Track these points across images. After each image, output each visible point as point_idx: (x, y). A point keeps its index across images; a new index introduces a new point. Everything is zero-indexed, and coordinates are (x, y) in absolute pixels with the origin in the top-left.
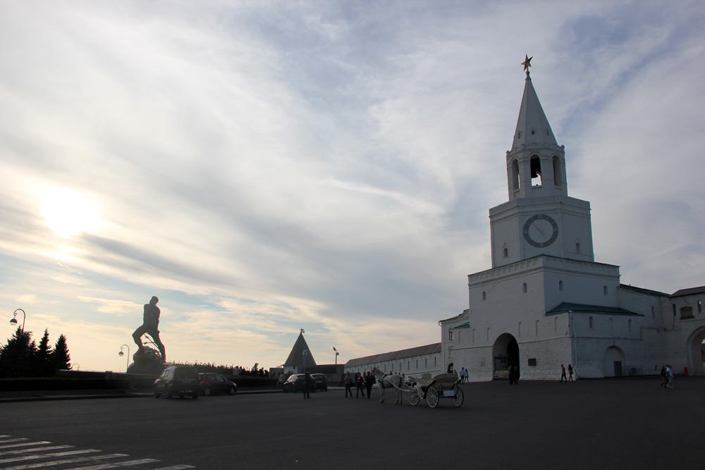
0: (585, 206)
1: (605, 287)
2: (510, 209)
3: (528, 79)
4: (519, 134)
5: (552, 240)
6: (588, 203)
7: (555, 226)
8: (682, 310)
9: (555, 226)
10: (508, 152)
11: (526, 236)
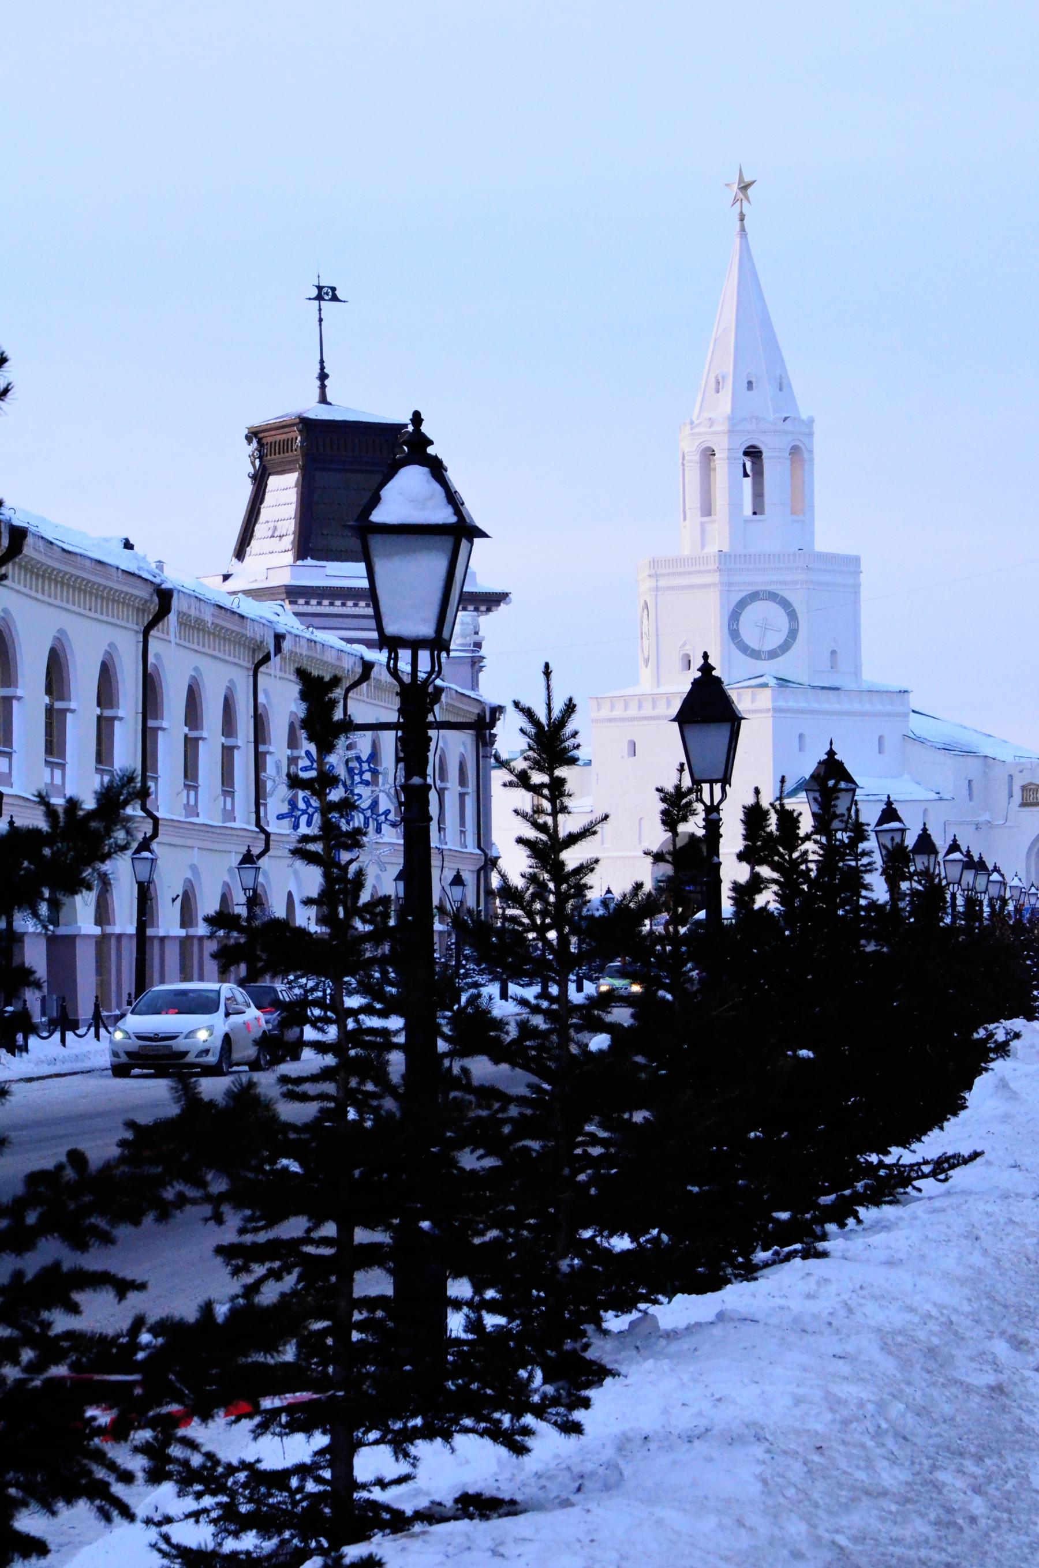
0: (851, 564)
1: (881, 738)
5: (785, 647)
6: (856, 560)
7: (792, 615)
8: (1024, 788)
9: (792, 615)
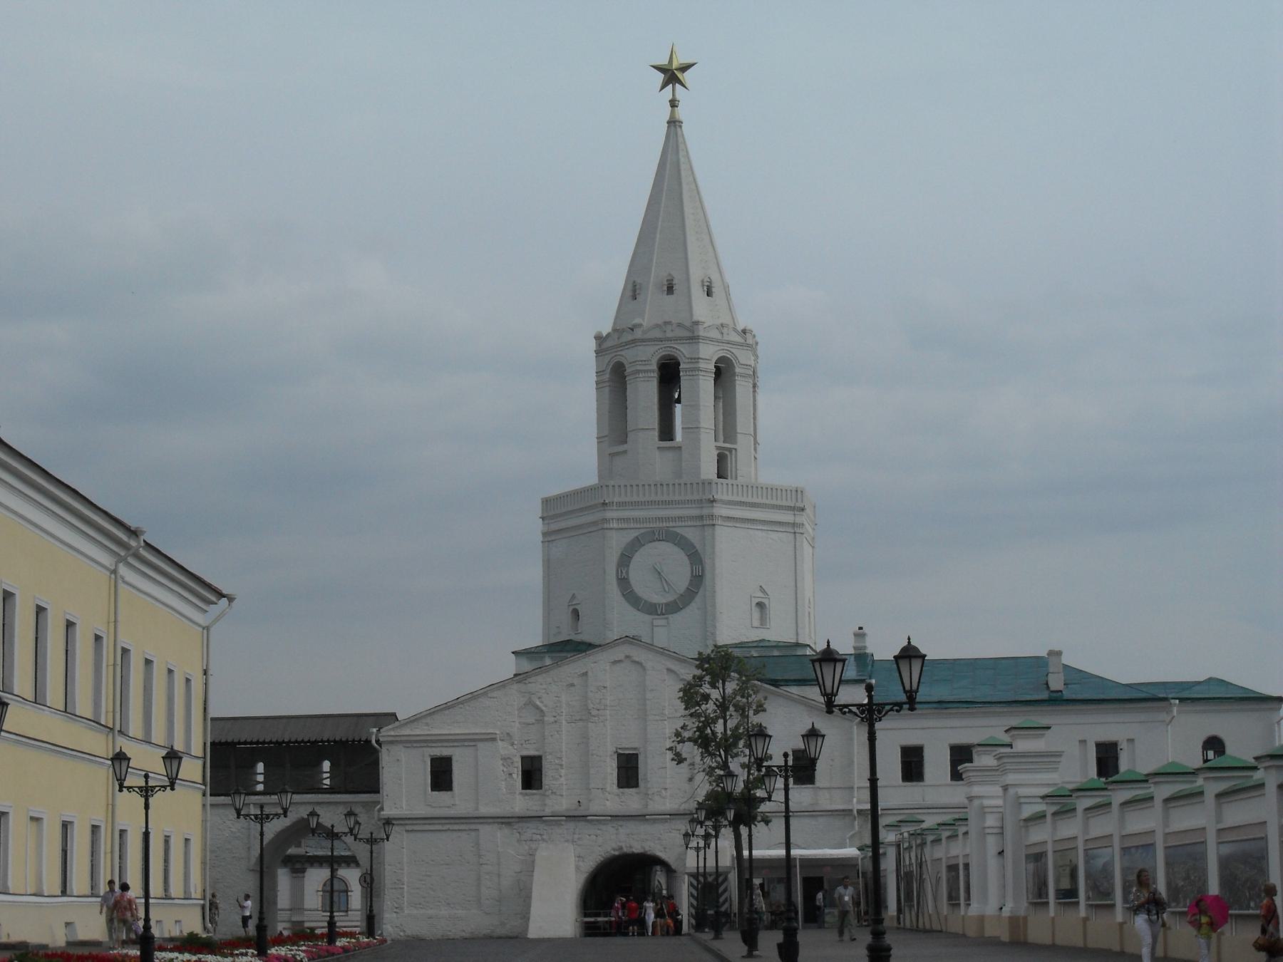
2: (581, 510)
3: (673, 123)
4: (634, 291)
10: (599, 338)
11: (624, 582)
